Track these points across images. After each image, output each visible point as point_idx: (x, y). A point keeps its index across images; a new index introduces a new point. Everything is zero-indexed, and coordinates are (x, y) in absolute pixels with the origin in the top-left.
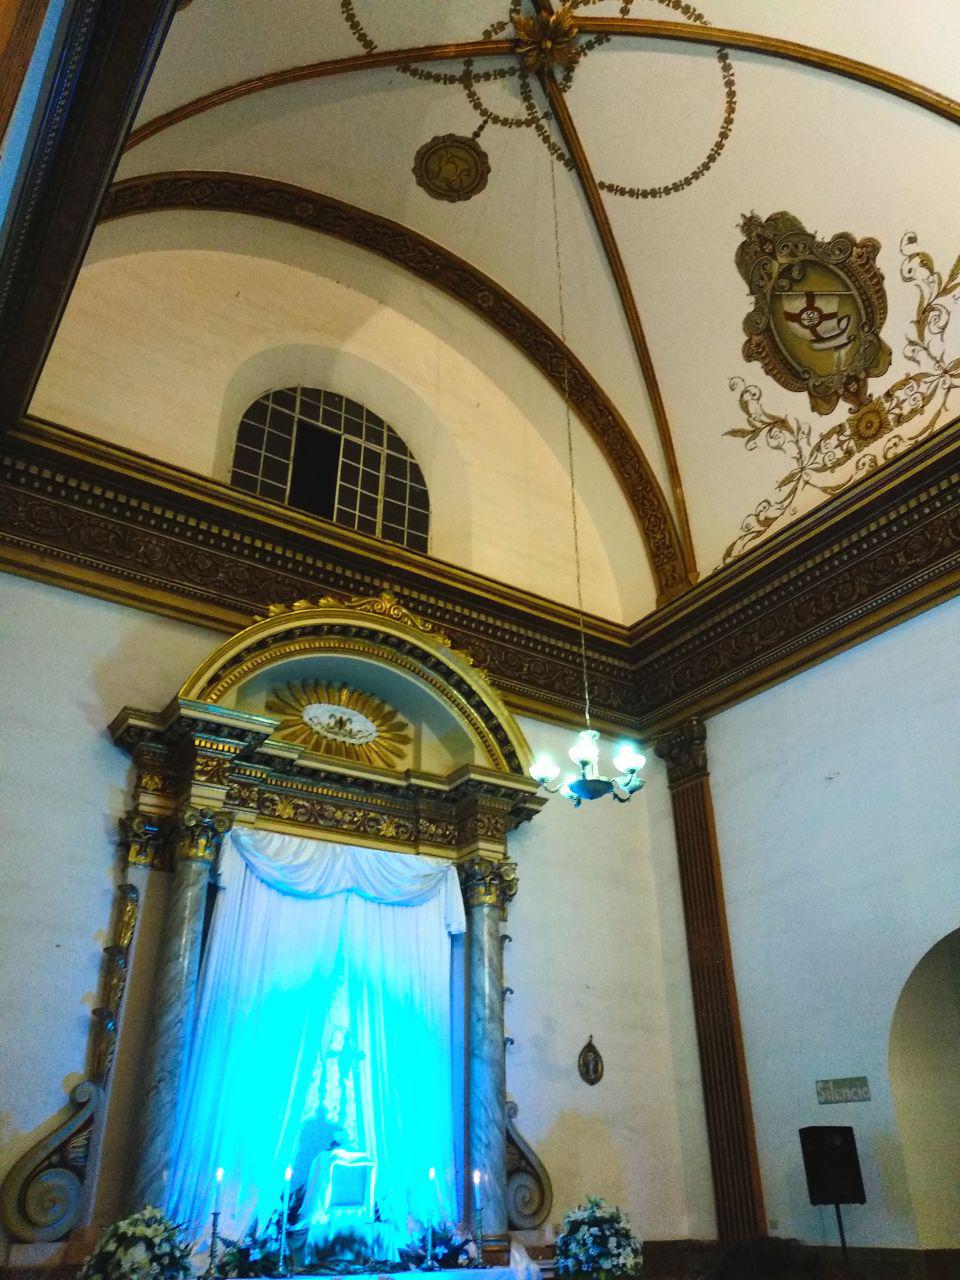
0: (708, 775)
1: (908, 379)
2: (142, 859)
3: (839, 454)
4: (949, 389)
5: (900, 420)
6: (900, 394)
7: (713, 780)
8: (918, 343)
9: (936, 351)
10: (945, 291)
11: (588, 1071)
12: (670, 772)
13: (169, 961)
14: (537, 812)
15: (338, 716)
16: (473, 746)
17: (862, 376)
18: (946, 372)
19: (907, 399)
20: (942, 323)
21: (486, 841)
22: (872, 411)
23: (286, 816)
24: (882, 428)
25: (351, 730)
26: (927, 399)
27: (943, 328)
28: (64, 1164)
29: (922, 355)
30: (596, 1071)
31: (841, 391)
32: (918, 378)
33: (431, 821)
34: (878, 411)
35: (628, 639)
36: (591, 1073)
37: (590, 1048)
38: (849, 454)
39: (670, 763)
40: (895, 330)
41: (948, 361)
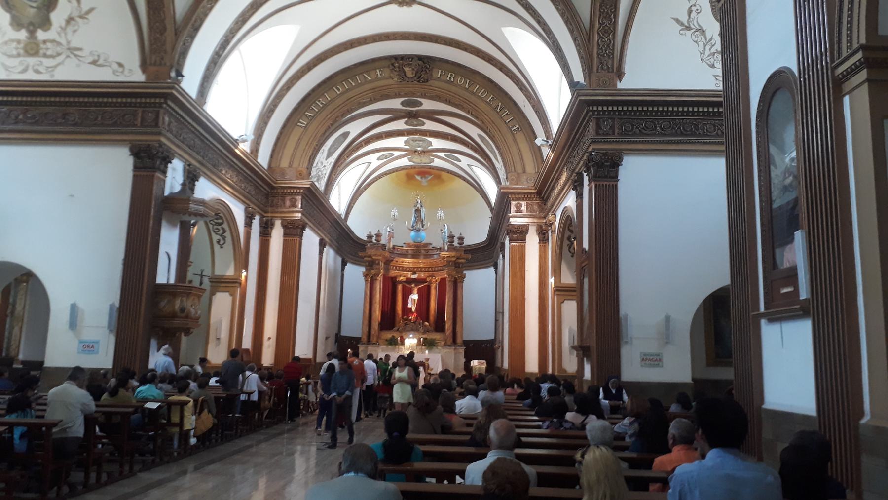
1: (53, 41)
3: (15, 53)
4: (68, 57)
5: (45, 56)
6: (49, 45)
8: (64, 29)
9: (70, 37)
10: (81, 17)
17: (37, 25)
18: (69, 49)
19: (51, 49)
20: (76, 28)
22: (35, 43)
24: (36, 53)
26: (59, 54)
27: (75, 31)
29: (63, 35)
31: (26, 25)
32: (59, 44)
34: (38, 45)
38: (19, 55)
40: (58, 17)
41: (73, 44)
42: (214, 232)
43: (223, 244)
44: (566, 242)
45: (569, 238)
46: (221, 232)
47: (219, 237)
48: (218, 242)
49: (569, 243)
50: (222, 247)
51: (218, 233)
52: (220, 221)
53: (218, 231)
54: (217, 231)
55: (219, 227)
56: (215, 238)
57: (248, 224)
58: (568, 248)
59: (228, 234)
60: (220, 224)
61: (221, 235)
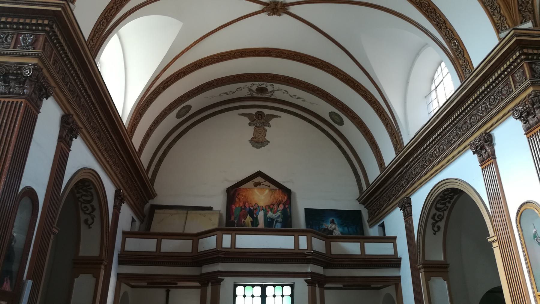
42: (82, 210)
43: (92, 223)
44: (431, 221)
45: (433, 218)
46: (90, 209)
47: (86, 217)
48: (86, 221)
49: (434, 221)
50: (90, 228)
51: (87, 212)
52: (89, 198)
53: (88, 210)
54: (86, 209)
55: (88, 206)
56: (83, 217)
57: (117, 208)
58: (432, 226)
59: (97, 213)
60: (89, 202)
61: (89, 214)
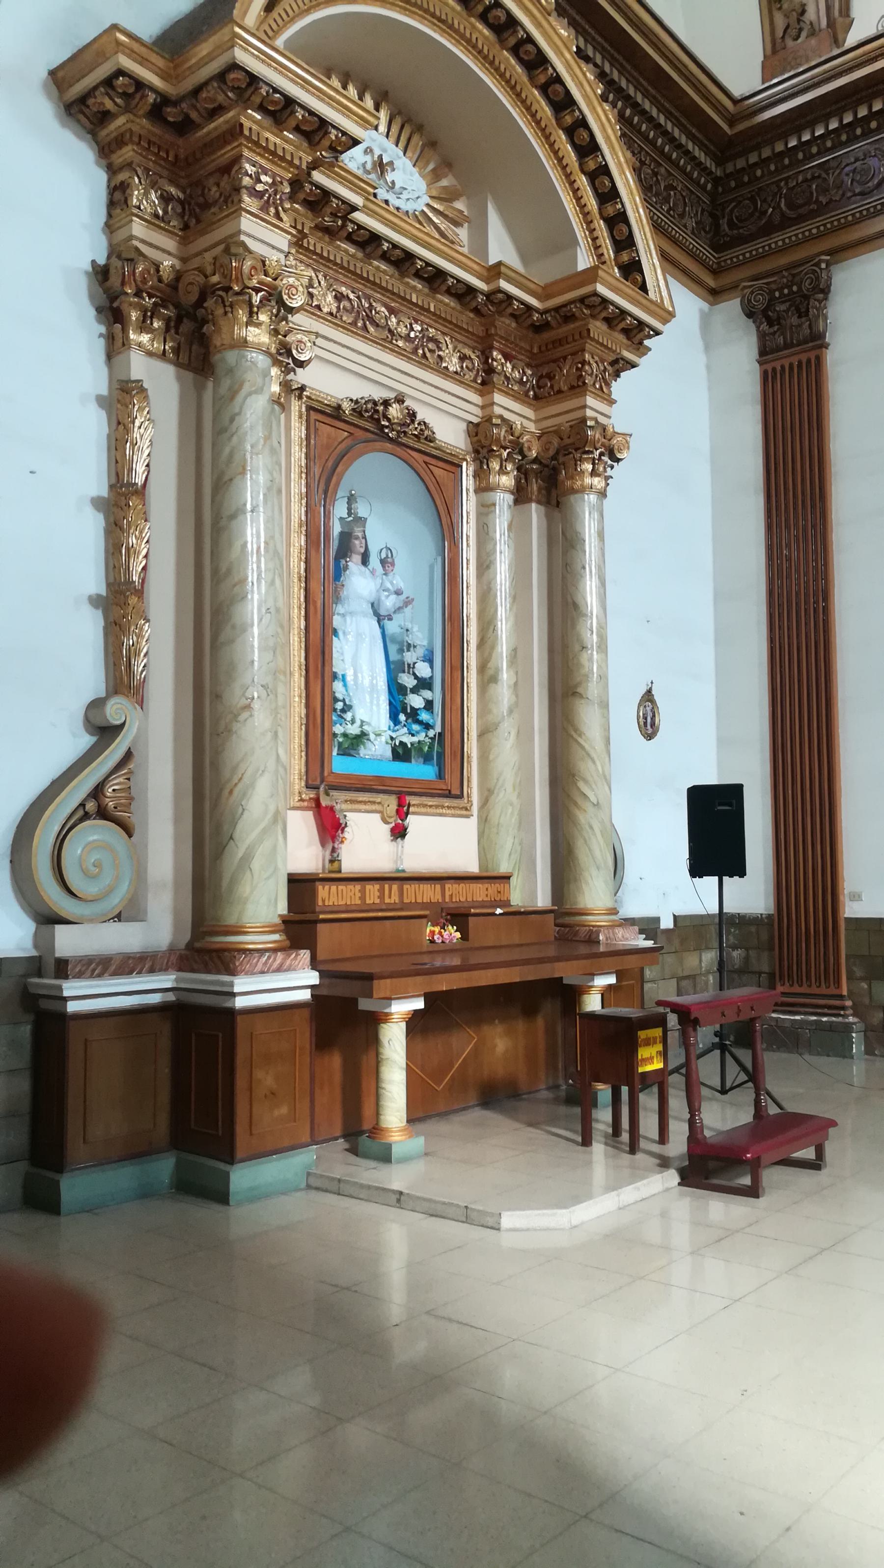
0: (826, 346)
2: (145, 338)
7: (831, 357)
11: (645, 724)
12: (762, 337)
13: (233, 517)
14: (633, 366)
15: (377, 152)
16: (576, 243)
21: (596, 396)
23: (326, 310)
25: (393, 182)
28: (103, 814)
30: (653, 725)
33: (507, 357)
35: (731, 123)
36: (649, 727)
37: (648, 697)
39: (764, 326)
